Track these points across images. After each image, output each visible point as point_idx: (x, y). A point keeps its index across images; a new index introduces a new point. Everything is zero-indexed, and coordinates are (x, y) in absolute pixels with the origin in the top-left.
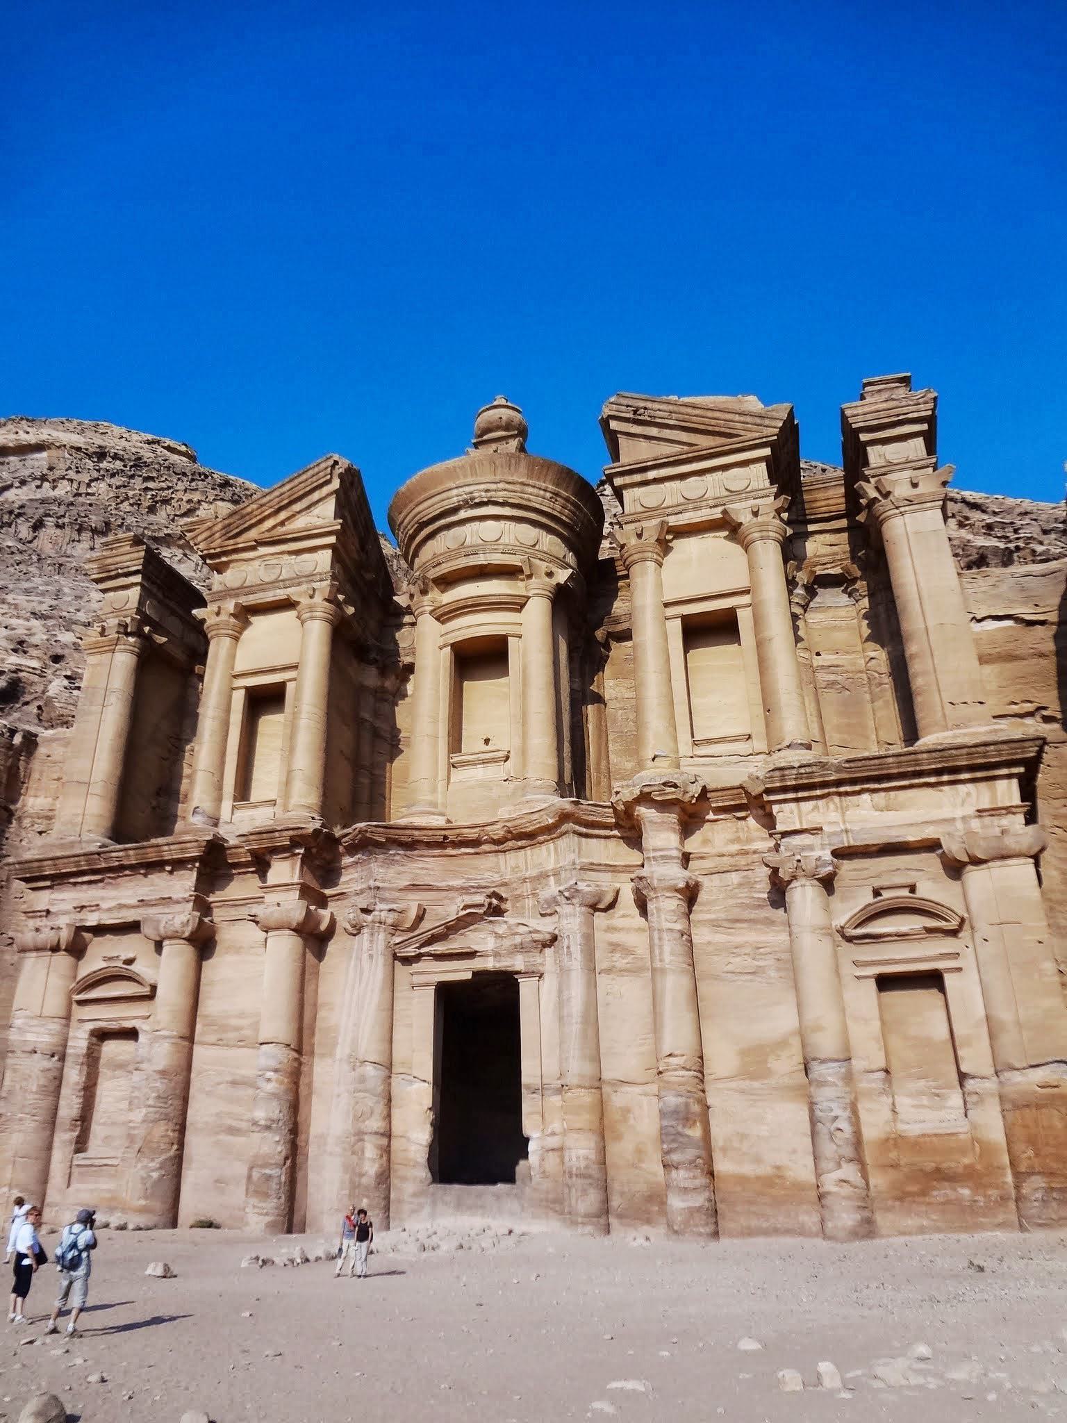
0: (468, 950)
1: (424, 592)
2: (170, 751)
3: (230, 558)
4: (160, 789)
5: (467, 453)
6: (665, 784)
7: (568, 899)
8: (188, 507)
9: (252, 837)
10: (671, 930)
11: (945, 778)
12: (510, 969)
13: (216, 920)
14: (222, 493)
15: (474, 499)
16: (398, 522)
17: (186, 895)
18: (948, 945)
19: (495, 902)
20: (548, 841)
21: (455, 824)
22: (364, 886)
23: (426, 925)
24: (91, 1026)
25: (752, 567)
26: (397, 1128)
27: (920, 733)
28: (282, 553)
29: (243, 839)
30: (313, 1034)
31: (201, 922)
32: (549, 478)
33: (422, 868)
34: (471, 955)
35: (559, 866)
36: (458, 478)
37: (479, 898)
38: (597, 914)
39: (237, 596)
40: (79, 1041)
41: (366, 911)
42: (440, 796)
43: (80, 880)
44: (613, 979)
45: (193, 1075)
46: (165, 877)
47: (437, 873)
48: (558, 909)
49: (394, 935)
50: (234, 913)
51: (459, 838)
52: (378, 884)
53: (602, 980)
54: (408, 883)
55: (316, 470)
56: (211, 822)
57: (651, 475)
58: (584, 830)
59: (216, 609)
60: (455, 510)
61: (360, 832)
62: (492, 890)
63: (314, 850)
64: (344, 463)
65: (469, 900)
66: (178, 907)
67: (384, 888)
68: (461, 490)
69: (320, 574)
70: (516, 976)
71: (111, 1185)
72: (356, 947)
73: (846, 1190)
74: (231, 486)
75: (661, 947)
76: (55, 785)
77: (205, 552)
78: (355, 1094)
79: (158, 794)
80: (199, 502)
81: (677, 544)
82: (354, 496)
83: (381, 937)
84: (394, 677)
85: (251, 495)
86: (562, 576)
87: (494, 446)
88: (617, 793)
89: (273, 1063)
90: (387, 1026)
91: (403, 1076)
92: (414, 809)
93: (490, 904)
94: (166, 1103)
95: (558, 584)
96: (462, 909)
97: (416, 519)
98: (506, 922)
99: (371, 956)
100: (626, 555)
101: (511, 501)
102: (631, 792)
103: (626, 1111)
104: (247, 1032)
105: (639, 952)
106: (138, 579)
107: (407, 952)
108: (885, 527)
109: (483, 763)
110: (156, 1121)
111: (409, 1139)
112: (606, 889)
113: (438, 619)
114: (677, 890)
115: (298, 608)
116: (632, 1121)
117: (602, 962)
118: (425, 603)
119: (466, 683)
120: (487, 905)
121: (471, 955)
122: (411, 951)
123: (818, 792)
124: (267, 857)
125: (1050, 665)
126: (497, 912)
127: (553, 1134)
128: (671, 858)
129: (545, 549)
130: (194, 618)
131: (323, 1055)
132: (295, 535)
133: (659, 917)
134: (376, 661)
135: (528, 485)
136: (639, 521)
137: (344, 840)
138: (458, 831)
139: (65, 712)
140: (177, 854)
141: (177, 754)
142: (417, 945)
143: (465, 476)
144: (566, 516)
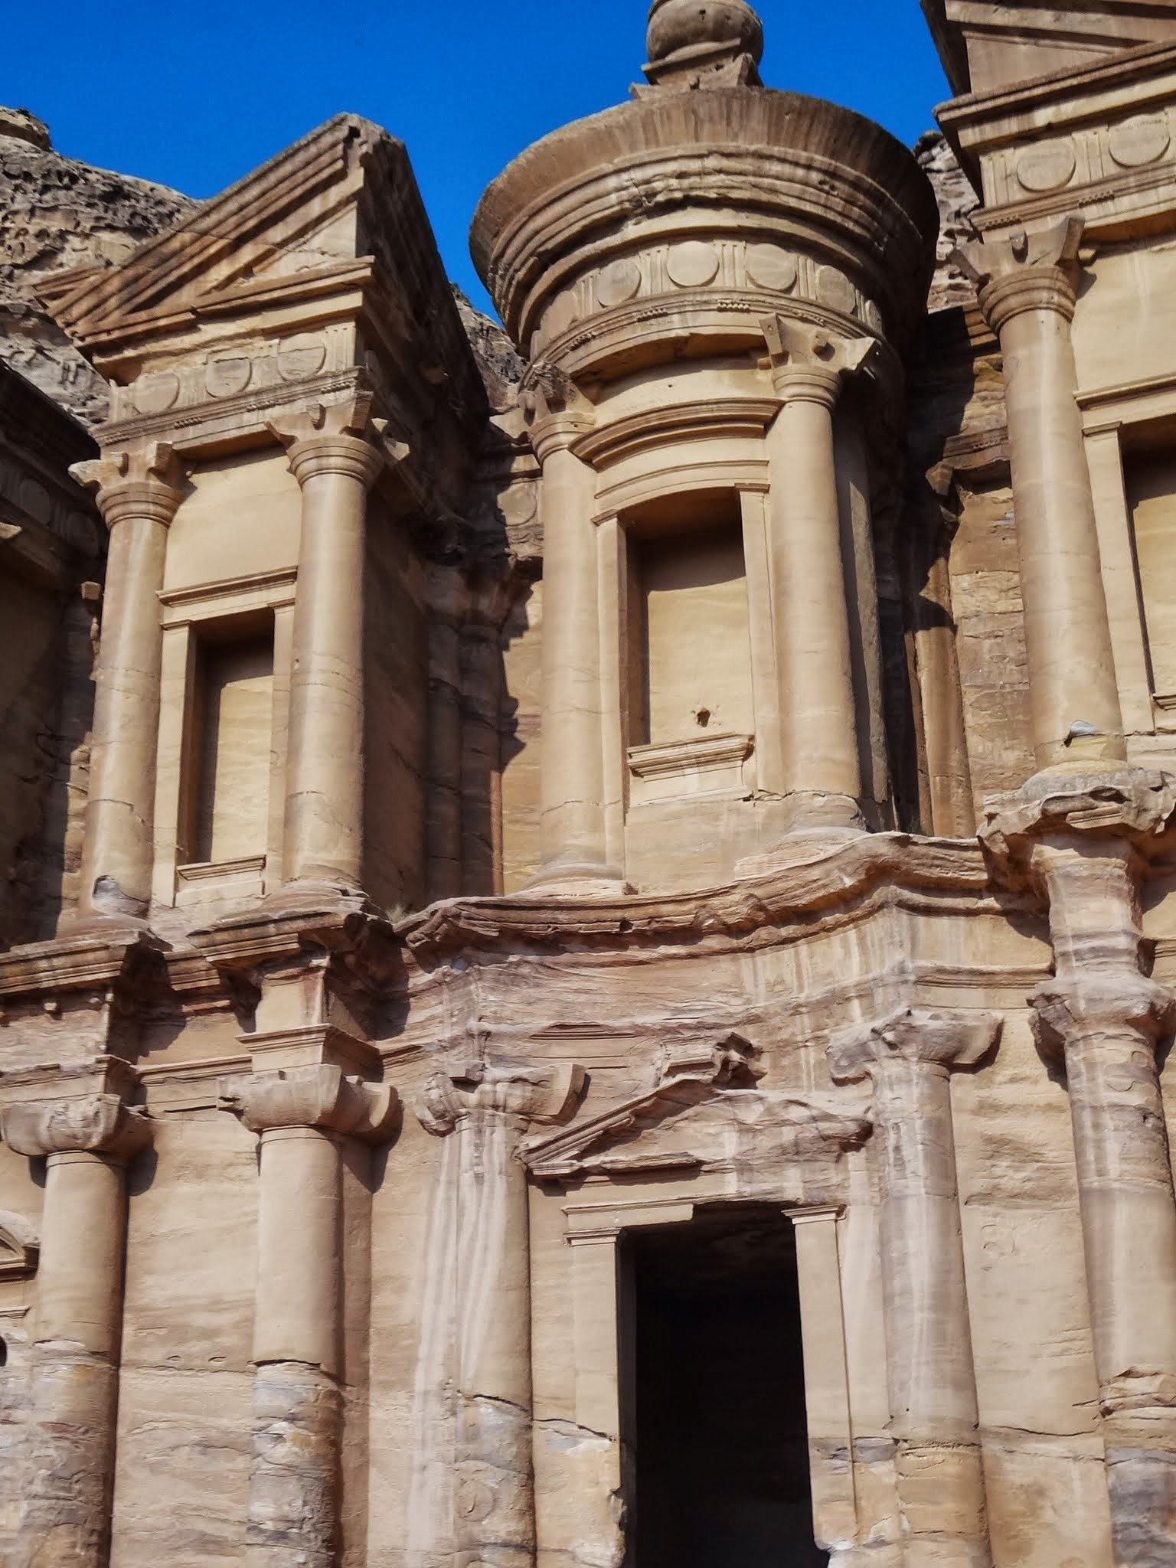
0: (683, 1160)
1: (556, 404)
2: (38, 763)
3: (142, 350)
4: (22, 843)
5: (634, 96)
6: (1095, 794)
7: (892, 1046)
8: (40, 246)
9: (219, 937)
10: (1120, 1107)
12: (772, 1198)
13: (154, 1109)
14: (110, 215)
15: (655, 194)
16: (493, 255)
17: (91, 1060)
19: (735, 1056)
20: (846, 924)
21: (642, 896)
22: (457, 1031)
23: (592, 1109)
26: (549, 1532)
28: (251, 334)
29: (203, 940)
30: (365, 1341)
31: (123, 1113)
32: (815, 139)
33: (577, 991)
34: (690, 1169)
35: (870, 976)
36: (618, 151)
37: (703, 1051)
38: (956, 1077)
39: (161, 430)
41: (465, 1083)
42: (608, 837)
44: (996, 1215)
45: (121, 1431)
46: (47, 1025)
47: (608, 999)
48: (871, 1068)
49: (524, 1132)
50: (190, 1095)
51: (654, 925)
52: (487, 1026)
53: (973, 1218)
54: (552, 1022)
55: (313, 150)
56: (135, 907)
57: (1043, 117)
58: (919, 899)
59: (118, 461)
60: (614, 223)
61: (445, 918)
62: (729, 1031)
63: (350, 959)
64: (372, 132)
65: (681, 1053)
66: (75, 1087)
67: (500, 1035)
68: (625, 176)
69: (335, 376)
70: (787, 1213)
72: (446, 1159)
74: (128, 197)
75: (1099, 1144)
77: (89, 340)
78: (457, 1466)
79: (19, 853)
80: (62, 235)
81: (1104, 268)
82: (395, 203)
83: (499, 1137)
84: (496, 589)
85: (171, 215)
86: (852, 353)
87: (690, 77)
88: (991, 817)
89: (285, 1403)
90: (518, 1327)
91: (556, 1425)
93: (726, 1062)
94: (69, 1490)
95: (844, 373)
96: (667, 1075)
97: (531, 245)
98: (760, 1099)
99: (479, 1178)
100: (992, 299)
101: (735, 194)
102: (1021, 815)
104: (226, 1341)
105: (1050, 1155)
107: (553, 1166)
109: (699, 764)
110: (50, 1527)
111: (574, 1558)
112: (974, 1023)
113: (587, 460)
114: (1134, 1022)
115: (294, 449)
116: (1048, 1515)
117: (971, 1179)
118: (559, 428)
119: (653, 595)
120: (718, 1064)
121: (690, 1169)
122: (562, 1164)
124: (254, 977)
126: (743, 1077)
127: (880, 1543)
128: (1114, 952)
129: (812, 297)
130: (74, 481)
131: (387, 1386)
132: (276, 294)
133: (1092, 1079)
134: (455, 558)
135: (770, 157)
136: (1018, 222)
137: (411, 936)
138: (651, 910)
140: (66, 975)
141: (55, 770)
142: (575, 1152)
143: (633, 147)
144: (856, 222)
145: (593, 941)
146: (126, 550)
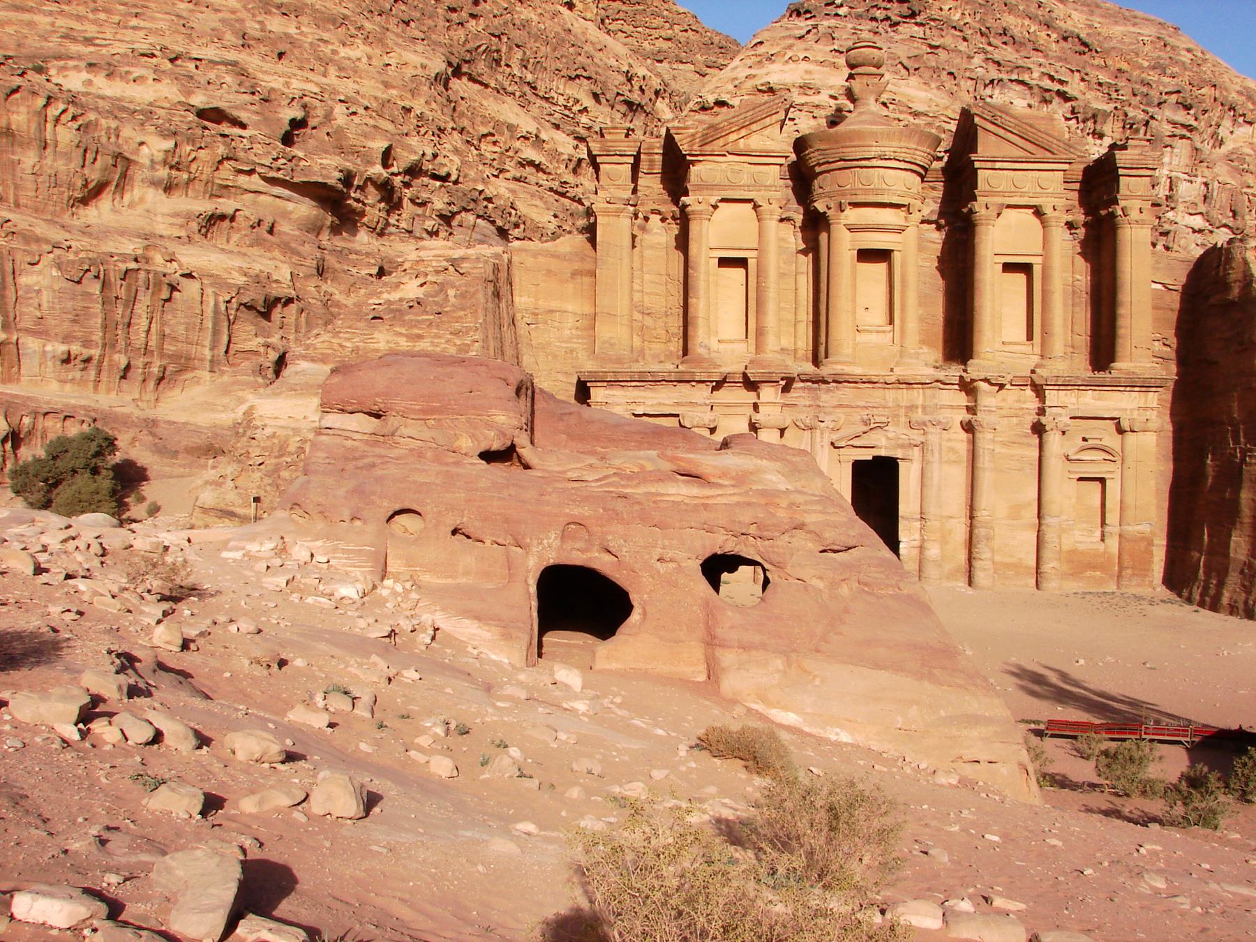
11: (1128, 389)
18: (1110, 466)
22: (811, 403)
27: (1117, 359)
37: (884, 419)
43: (629, 384)
50: (727, 410)
57: (998, 165)
73: (1054, 571)
76: (533, 288)
81: (1006, 212)
87: (865, 79)
108: (1120, 232)
122: (843, 444)
123: (1070, 388)
139: (358, 143)
146: (701, 231)
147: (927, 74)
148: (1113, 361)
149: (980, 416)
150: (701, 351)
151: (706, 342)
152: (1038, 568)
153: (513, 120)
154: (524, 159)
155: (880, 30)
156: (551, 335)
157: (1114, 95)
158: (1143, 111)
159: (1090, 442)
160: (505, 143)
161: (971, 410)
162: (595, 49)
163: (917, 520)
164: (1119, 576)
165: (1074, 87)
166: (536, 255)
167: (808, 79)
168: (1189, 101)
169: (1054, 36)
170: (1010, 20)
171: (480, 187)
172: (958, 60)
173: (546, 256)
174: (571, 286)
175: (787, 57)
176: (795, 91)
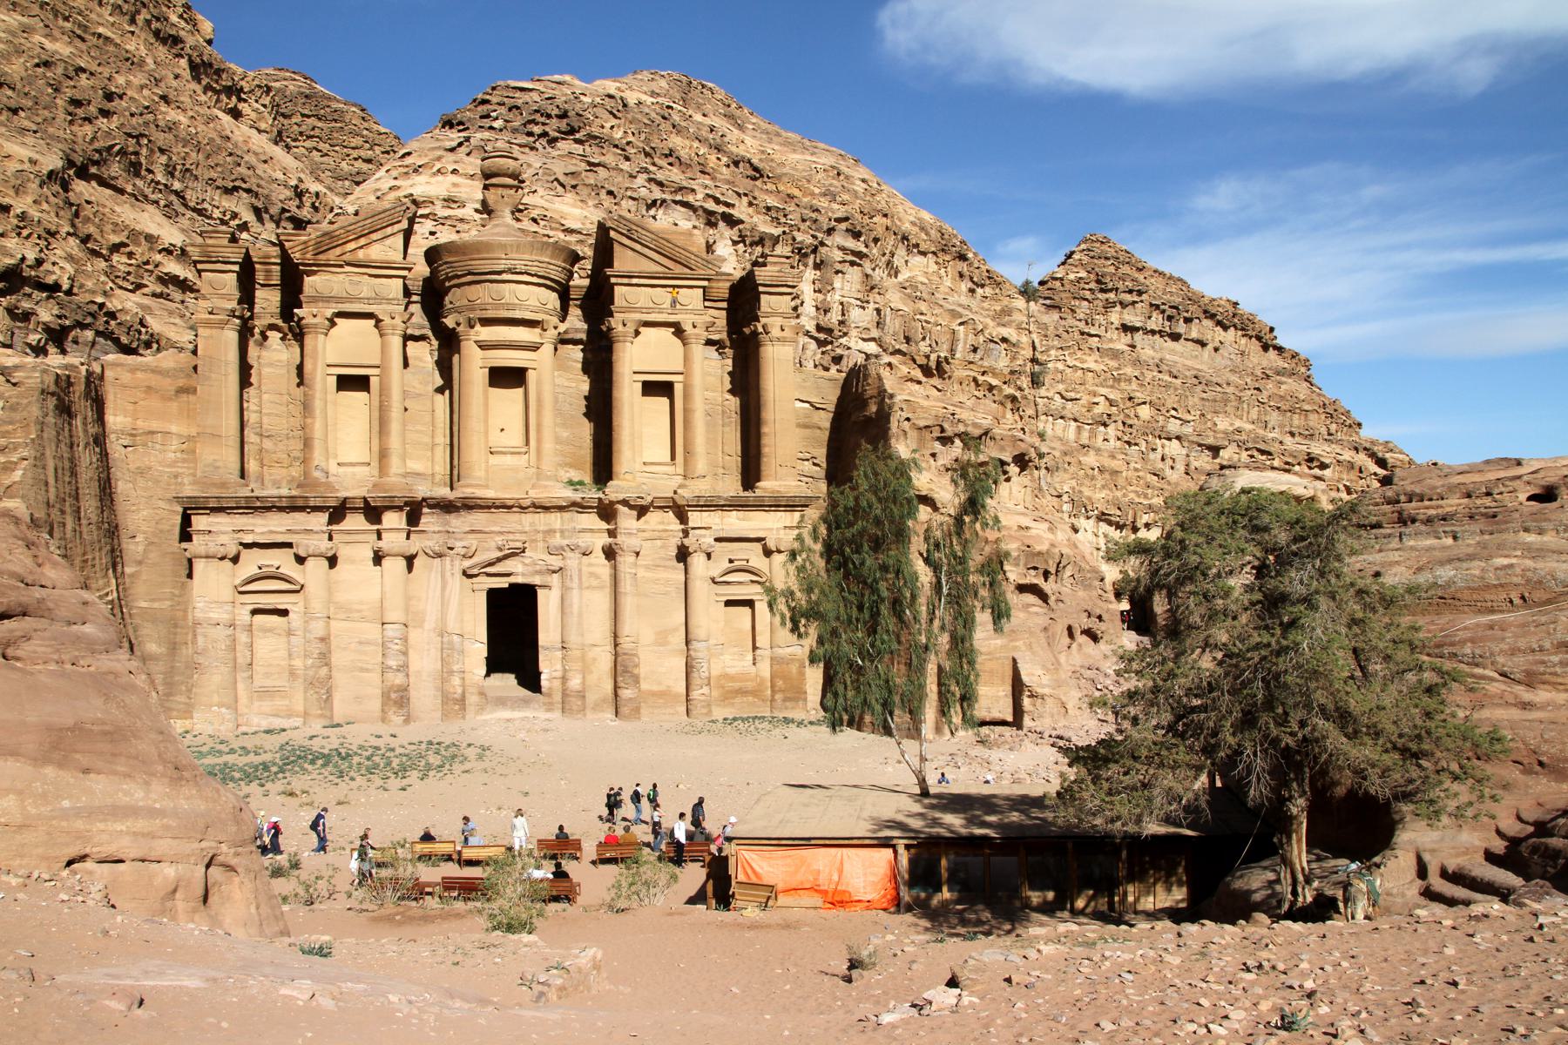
1: (472, 327)
17: (325, 528)
24: (251, 607)
25: (687, 359)
34: (508, 575)
37: (519, 545)
40: (244, 615)
57: (635, 281)
60: (499, 273)
66: (316, 536)
71: (287, 702)
76: (130, 407)
81: (642, 329)
83: (457, 562)
87: (500, 191)
92: (469, 481)
103: (594, 659)
106: (236, 268)
113: (480, 347)
117: (585, 584)
121: (508, 575)
122: (475, 571)
125: (825, 436)
145: (482, 507)
146: (316, 346)
147: (584, 191)
148: (759, 480)
149: (620, 539)
150: (317, 474)
151: (323, 464)
152: (687, 695)
153: (153, 230)
154: (166, 274)
155: (538, 145)
156: (152, 459)
157: (783, 220)
158: (813, 236)
159: (736, 563)
160: (143, 254)
161: (612, 533)
162: (258, 160)
163: (558, 650)
164: (773, 700)
165: (741, 210)
166: (133, 370)
167: (455, 193)
168: (858, 228)
169: (725, 159)
170: (676, 141)
171: (100, 300)
172: (620, 179)
173: (145, 371)
174: (175, 404)
175: (435, 169)
176: (439, 204)
